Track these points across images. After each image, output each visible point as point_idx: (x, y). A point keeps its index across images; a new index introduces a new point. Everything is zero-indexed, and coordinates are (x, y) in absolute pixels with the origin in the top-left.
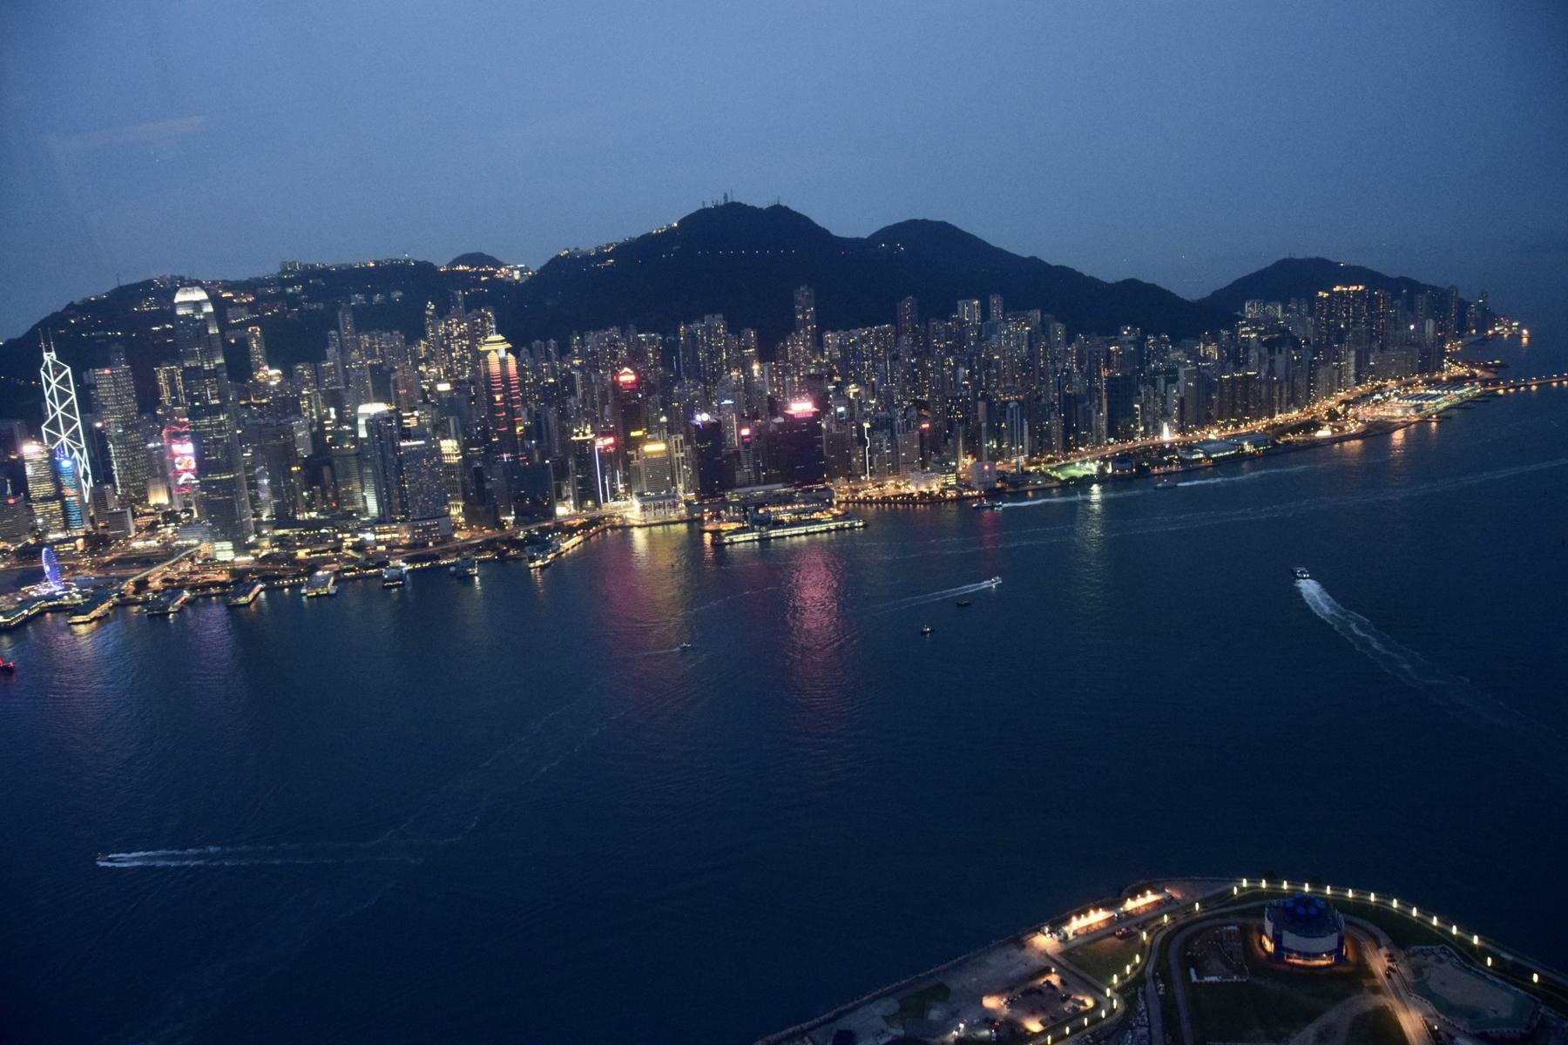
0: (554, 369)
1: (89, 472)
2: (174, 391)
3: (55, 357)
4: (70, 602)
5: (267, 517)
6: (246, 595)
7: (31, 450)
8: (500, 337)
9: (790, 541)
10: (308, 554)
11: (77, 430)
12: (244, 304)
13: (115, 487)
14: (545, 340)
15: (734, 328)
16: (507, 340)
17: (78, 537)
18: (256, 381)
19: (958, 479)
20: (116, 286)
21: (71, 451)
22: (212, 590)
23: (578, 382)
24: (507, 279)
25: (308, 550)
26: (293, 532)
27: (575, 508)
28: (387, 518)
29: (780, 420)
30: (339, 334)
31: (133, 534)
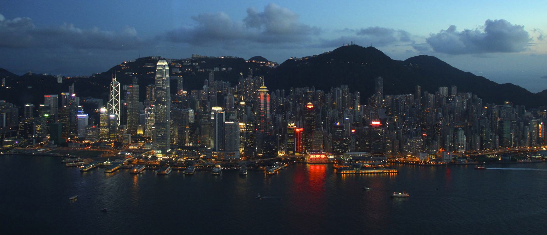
0: (283, 100)
1: (120, 120)
2: (151, 96)
3: (115, 80)
4: (106, 165)
5: (175, 143)
7: (103, 110)
8: (265, 87)
9: (368, 176)
10: (187, 158)
11: (118, 105)
13: (127, 125)
14: (281, 90)
15: (352, 91)
16: (267, 88)
17: (112, 142)
18: (178, 95)
19: (436, 157)
20: (139, 58)
21: (115, 112)
23: (291, 105)
24: (270, 67)
25: (188, 157)
26: (184, 150)
27: (286, 153)
28: (217, 150)
29: (367, 127)
30: (208, 81)
31: (130, 144)
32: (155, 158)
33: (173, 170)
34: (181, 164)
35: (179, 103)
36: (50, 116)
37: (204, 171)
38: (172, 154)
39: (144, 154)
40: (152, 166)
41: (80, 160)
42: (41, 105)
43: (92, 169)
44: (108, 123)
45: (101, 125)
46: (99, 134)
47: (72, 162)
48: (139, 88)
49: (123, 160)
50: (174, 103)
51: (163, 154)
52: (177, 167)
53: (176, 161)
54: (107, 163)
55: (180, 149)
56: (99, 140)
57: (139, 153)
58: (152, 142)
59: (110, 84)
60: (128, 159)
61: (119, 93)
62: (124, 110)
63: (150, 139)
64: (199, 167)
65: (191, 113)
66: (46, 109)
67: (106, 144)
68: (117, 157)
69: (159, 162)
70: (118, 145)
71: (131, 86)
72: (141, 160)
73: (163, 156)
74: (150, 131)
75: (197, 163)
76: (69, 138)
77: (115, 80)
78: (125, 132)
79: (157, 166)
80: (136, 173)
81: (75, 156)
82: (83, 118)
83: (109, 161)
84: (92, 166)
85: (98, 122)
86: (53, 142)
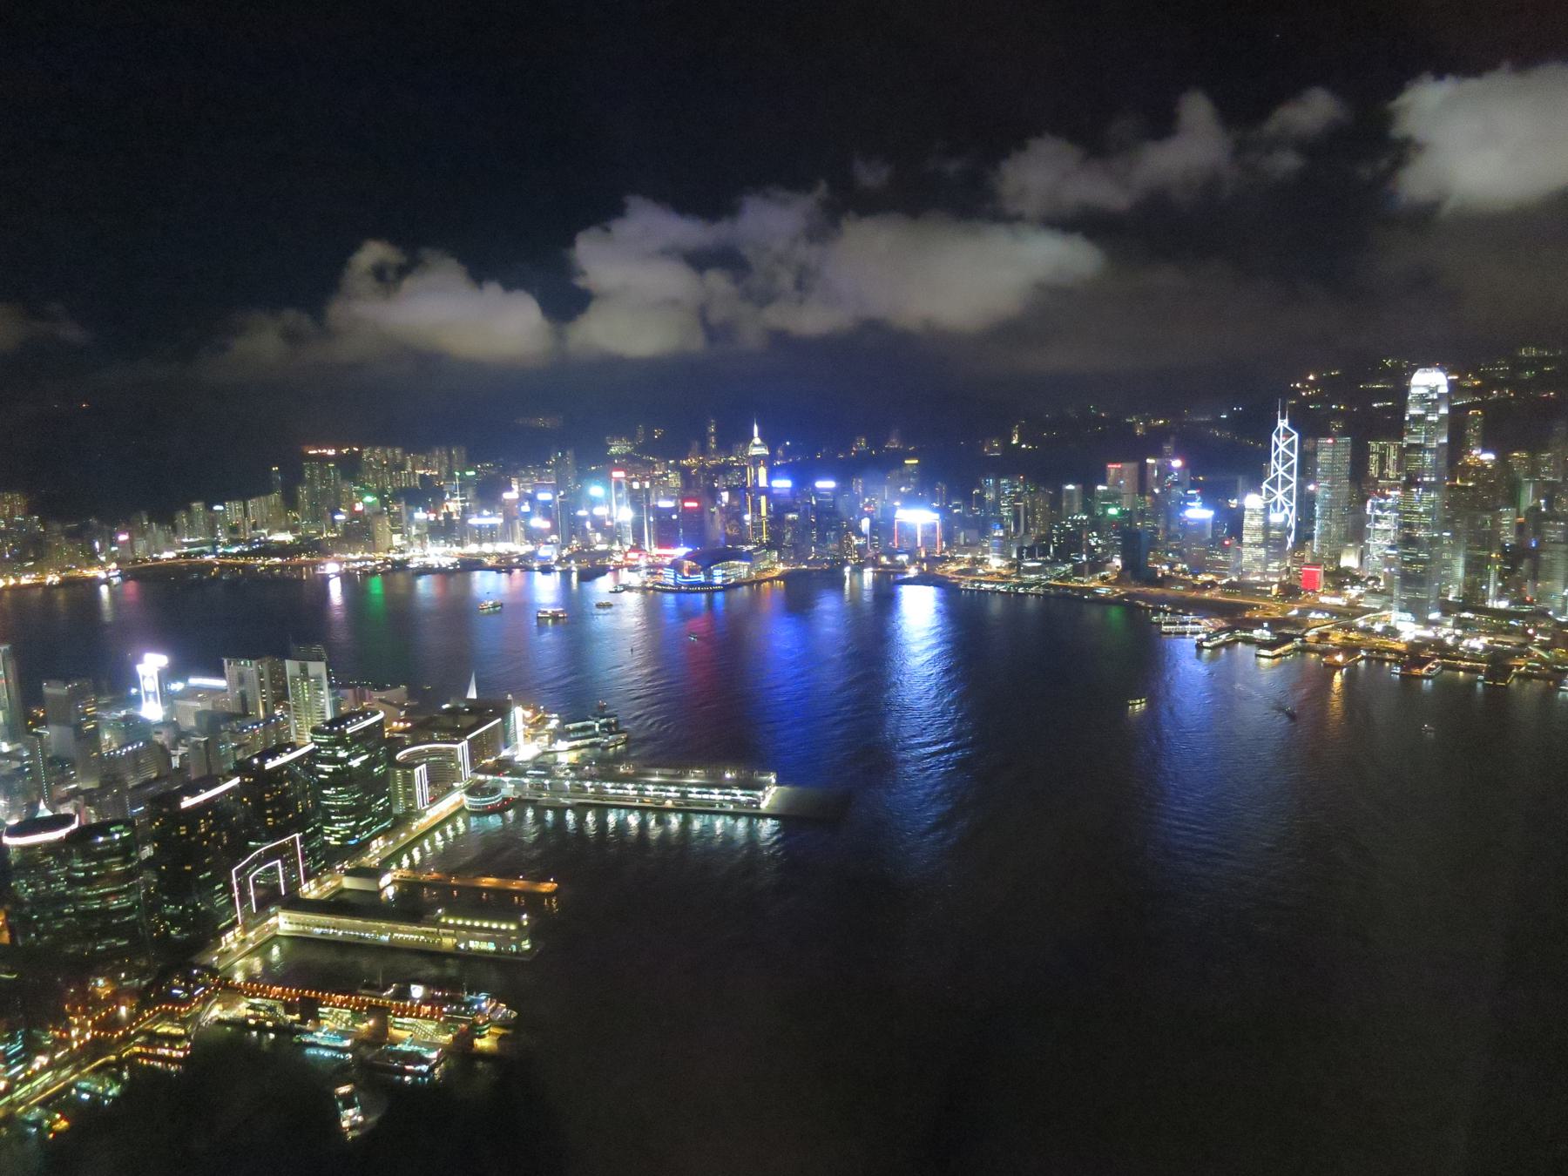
3: (1286, 426)
6: (1421, 667)
7: (1253, 501)
10: (1489, 641)
11: (1291, 490)
12: (1469, 388)
13: (1313, 544)
18: (1466, 463)
21: (1283, 508)
22: (1388, 656)
25: (1492, 639)
32: (1392, 632)
33: (1446, 667)
34: (1473, 655)
35: (1466, 488)
36: (1122, 513)
37: (1542, 682)
38: (1446, 626)
39: (1366, 620)
40: (1385, 652)
41: (1194, 621)
42: (1100, 488)
43: (1224, 644)
44: (1263, 534)
45: (1246, 539)
46: (1238, 561)
47: (1175, 624)
48: (1352, 446)
49: (1304, 630)
50: (1451, 488)
51: (1416, 622)
52: (1459, 662)
53: (1455, 648)
54: (1262, 635)
55: (1466, 615)
56: (1239, 577)
57: (1346, 615)
58: (1383, 590)
59: (1271, 437)
60: (1319, 628)
61: (1295, 461)
62: (1306, 504)
63: (1377, 580)
64: (1529, 667)
65: (1507, 519)
66: (1113, 498)
67: (1258, 588)
68: (1286, 622)
69: (1405, 643)
70: (1290, 591)
71: (1330, 441)
72: (1352, 635)
73: (1417, 629)
74: (1377, 559)
75: (1521, 656)
76: (1165, 568)
77: (1286, 426)
78: (1308, 560)
79: (1398, 652)
80: (1338, 667)
81: (1180, 611)
82: (1201, 524)
83: (1267, 629)
84: (1223, 637)
85: (1236, 529)
86: (1128, 574)
